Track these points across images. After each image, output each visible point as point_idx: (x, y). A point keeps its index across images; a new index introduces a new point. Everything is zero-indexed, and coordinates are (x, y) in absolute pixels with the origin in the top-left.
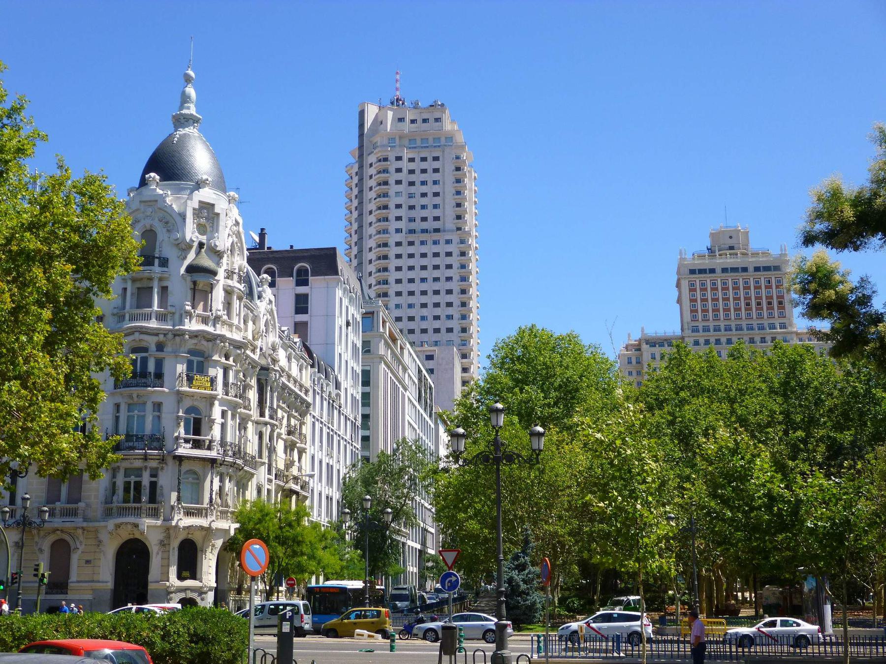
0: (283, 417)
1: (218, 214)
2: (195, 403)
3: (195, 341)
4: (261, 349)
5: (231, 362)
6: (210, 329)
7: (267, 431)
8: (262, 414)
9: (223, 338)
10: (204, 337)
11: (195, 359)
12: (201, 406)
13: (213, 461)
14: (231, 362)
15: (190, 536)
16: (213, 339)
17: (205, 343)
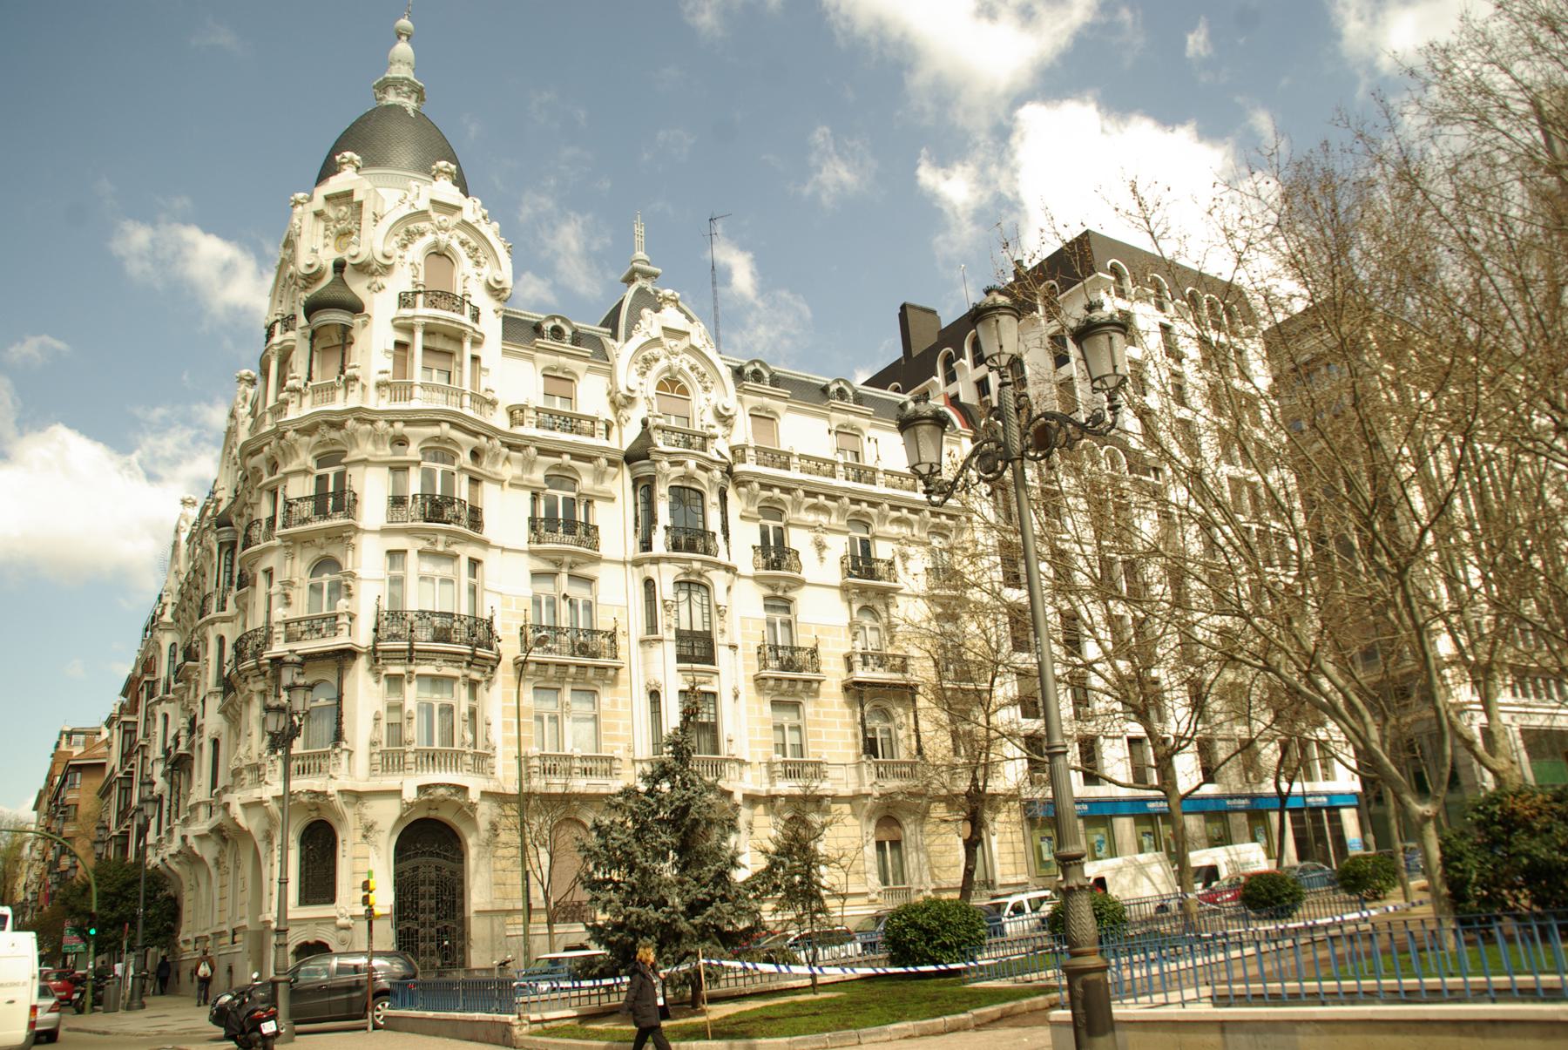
0: (820, 546)
1: (360, 204)
2: (323, 553)
3: (315, 438)
4: (645, 423)
5: (413, 452)
6: (340, 403)
7: (666, 577)
8: (647, 545)
9: (362, 415)
10: (335, 426)
11: (331, 472)
12: (334, 551)
13: (345, 656)
14: (413, 452)
15: (314, 814)
16: (335, 423)
17: (334, 434)
